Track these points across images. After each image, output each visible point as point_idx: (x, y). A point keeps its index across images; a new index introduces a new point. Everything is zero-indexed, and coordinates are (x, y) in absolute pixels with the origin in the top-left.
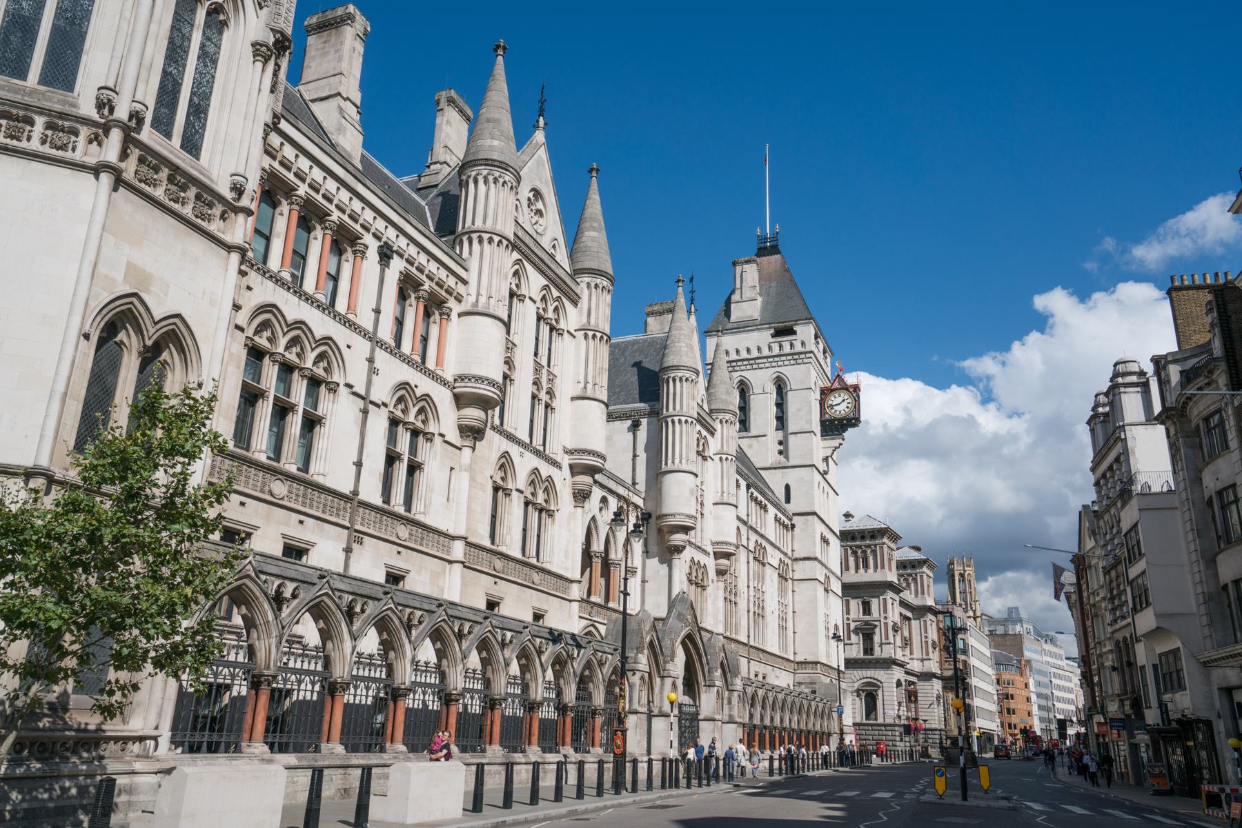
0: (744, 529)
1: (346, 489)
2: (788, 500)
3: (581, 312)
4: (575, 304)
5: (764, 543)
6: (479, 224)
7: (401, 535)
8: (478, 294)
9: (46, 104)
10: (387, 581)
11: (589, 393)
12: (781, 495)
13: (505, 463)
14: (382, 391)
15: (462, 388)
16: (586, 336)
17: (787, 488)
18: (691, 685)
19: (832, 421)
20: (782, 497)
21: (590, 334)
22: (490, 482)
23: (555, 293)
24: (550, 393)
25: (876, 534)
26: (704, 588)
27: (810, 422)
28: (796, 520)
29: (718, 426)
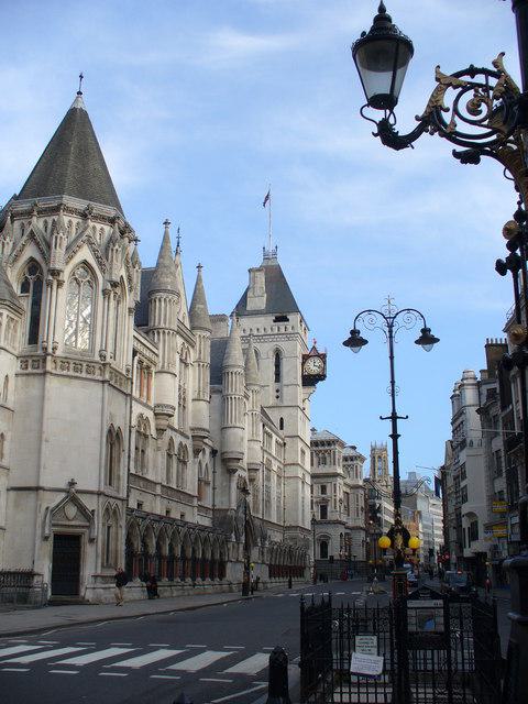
2: (282, 428)
4: (193, 347)
5: (271, 458)
6: (162, 325)
8: (164, 362)
9: (85, 358)
15: (158, 410)
18: (247, 548)
19: (310, 376)
20: (278, 424)
23: (186, 345)
24: (184, 399)
25: (329, 443)
27: (296, 378)
28: (287, 440)
29: (250, 394)
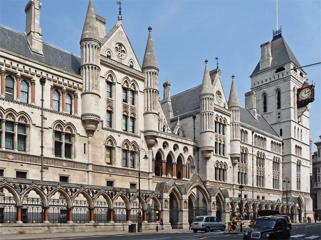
0: (250, 149)
1: (39, 154)
2: (281, 135)
3: (145, 83)
7: (64, 165)
10: (61, 180)
11: (149, 111)
12: (279, 133)
13: (111, 139)
14: (49, 123)
16: (147, 92)
17: (281, 130)
21: (149, 90)
22: (104, 146)
23: (131, 79)
24: (134, 114)
26: (226, 170)
28: (284, 142)
